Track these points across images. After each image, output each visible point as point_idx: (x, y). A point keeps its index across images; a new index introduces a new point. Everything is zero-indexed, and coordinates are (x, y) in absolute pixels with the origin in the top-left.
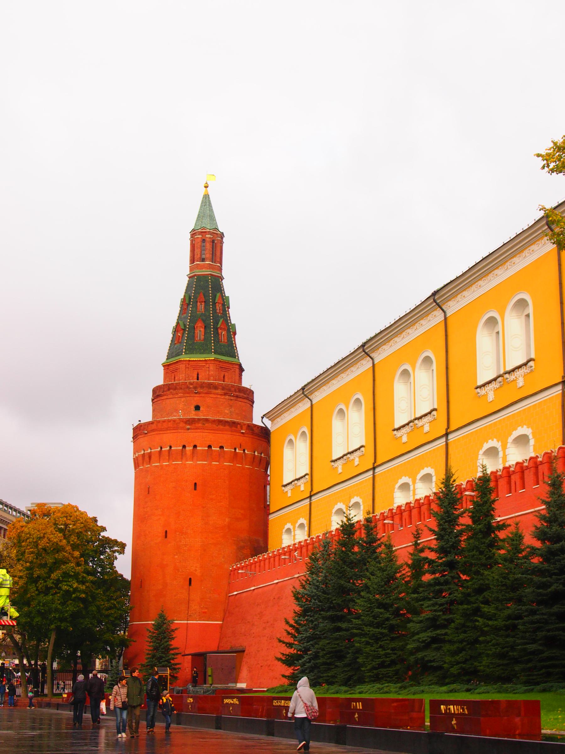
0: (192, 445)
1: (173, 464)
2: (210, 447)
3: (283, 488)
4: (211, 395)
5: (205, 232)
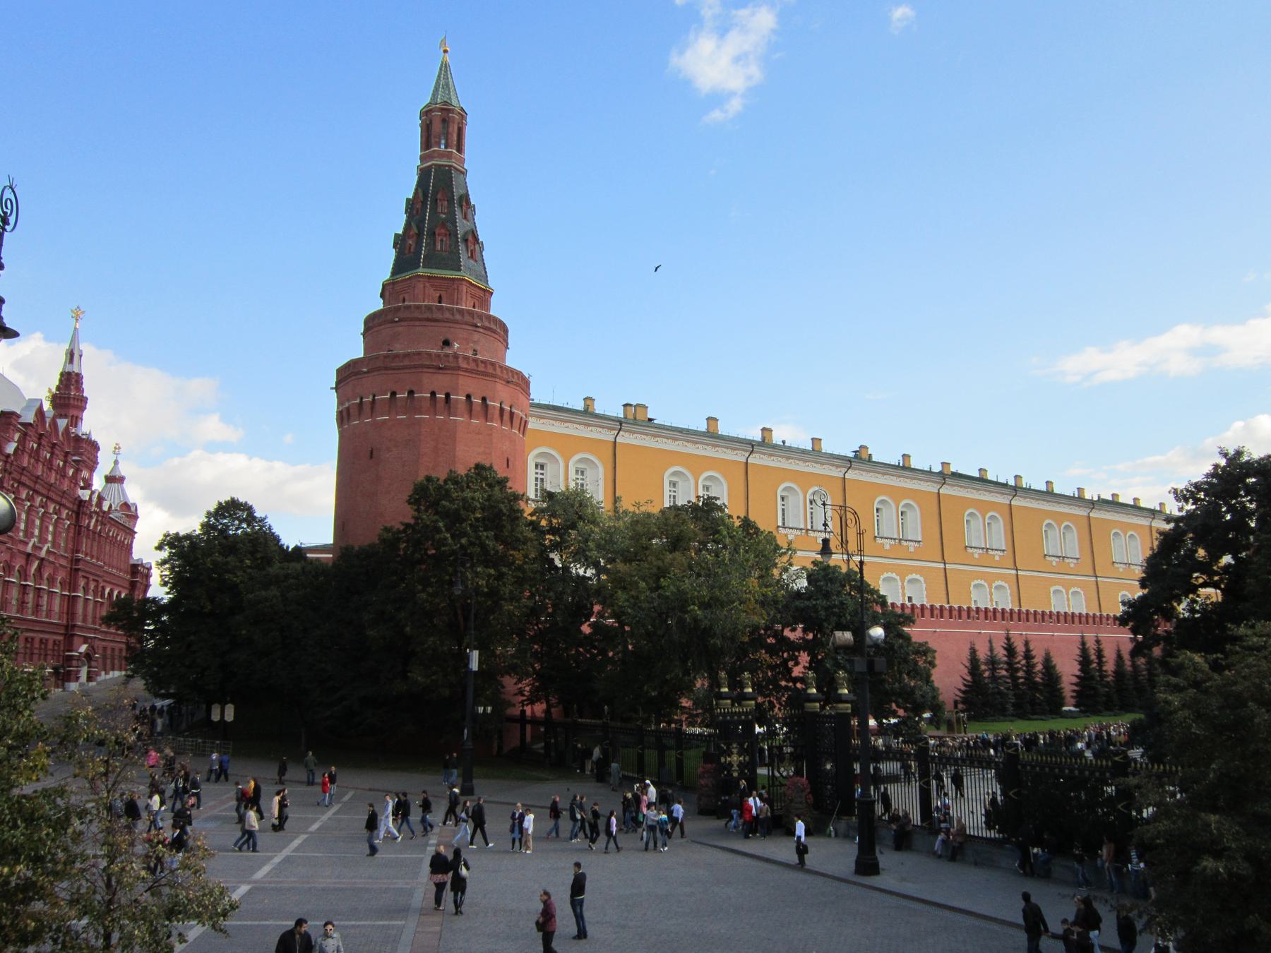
5: (449, 110)
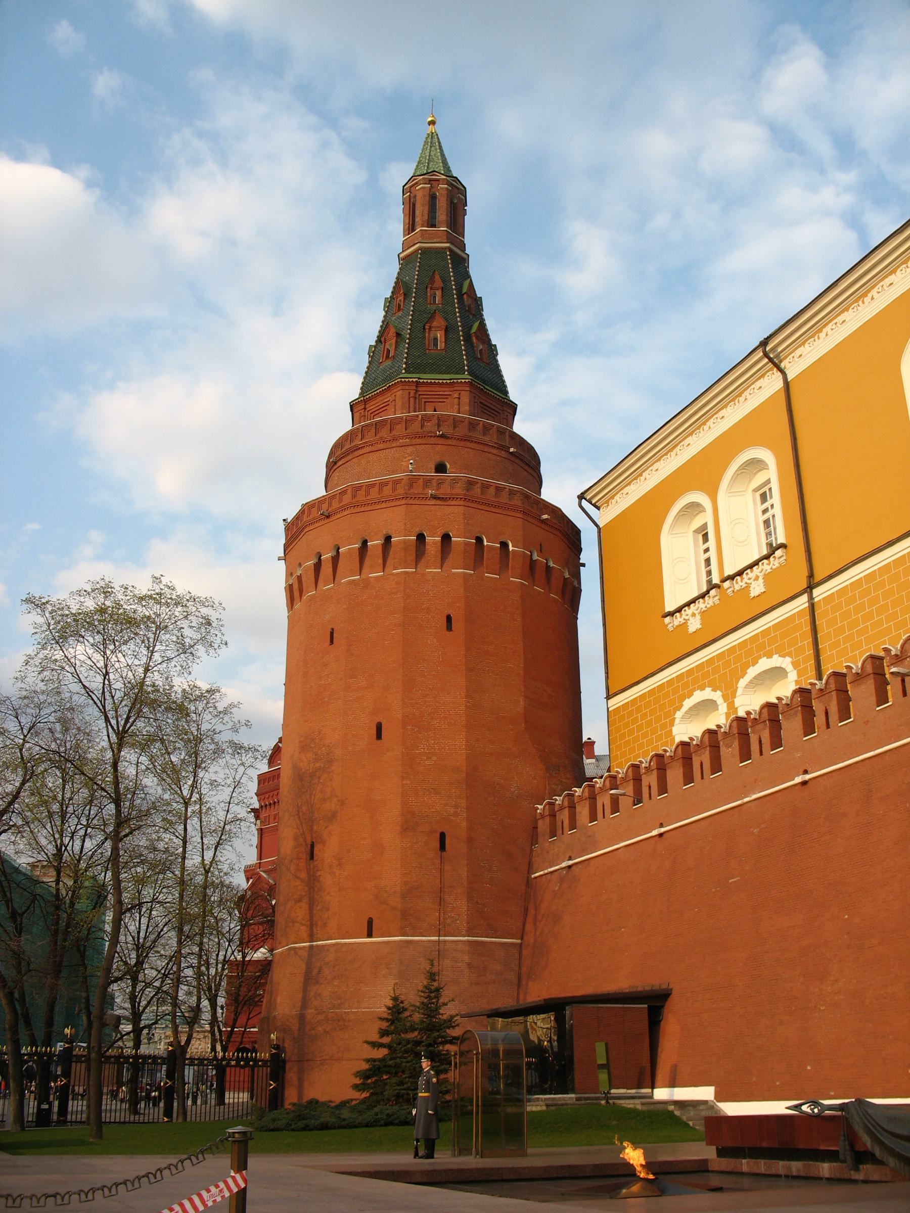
0: (441, 532)
1: (393, 575)
2: (479, 540)
3: (667, 620)
4: (468, 444)
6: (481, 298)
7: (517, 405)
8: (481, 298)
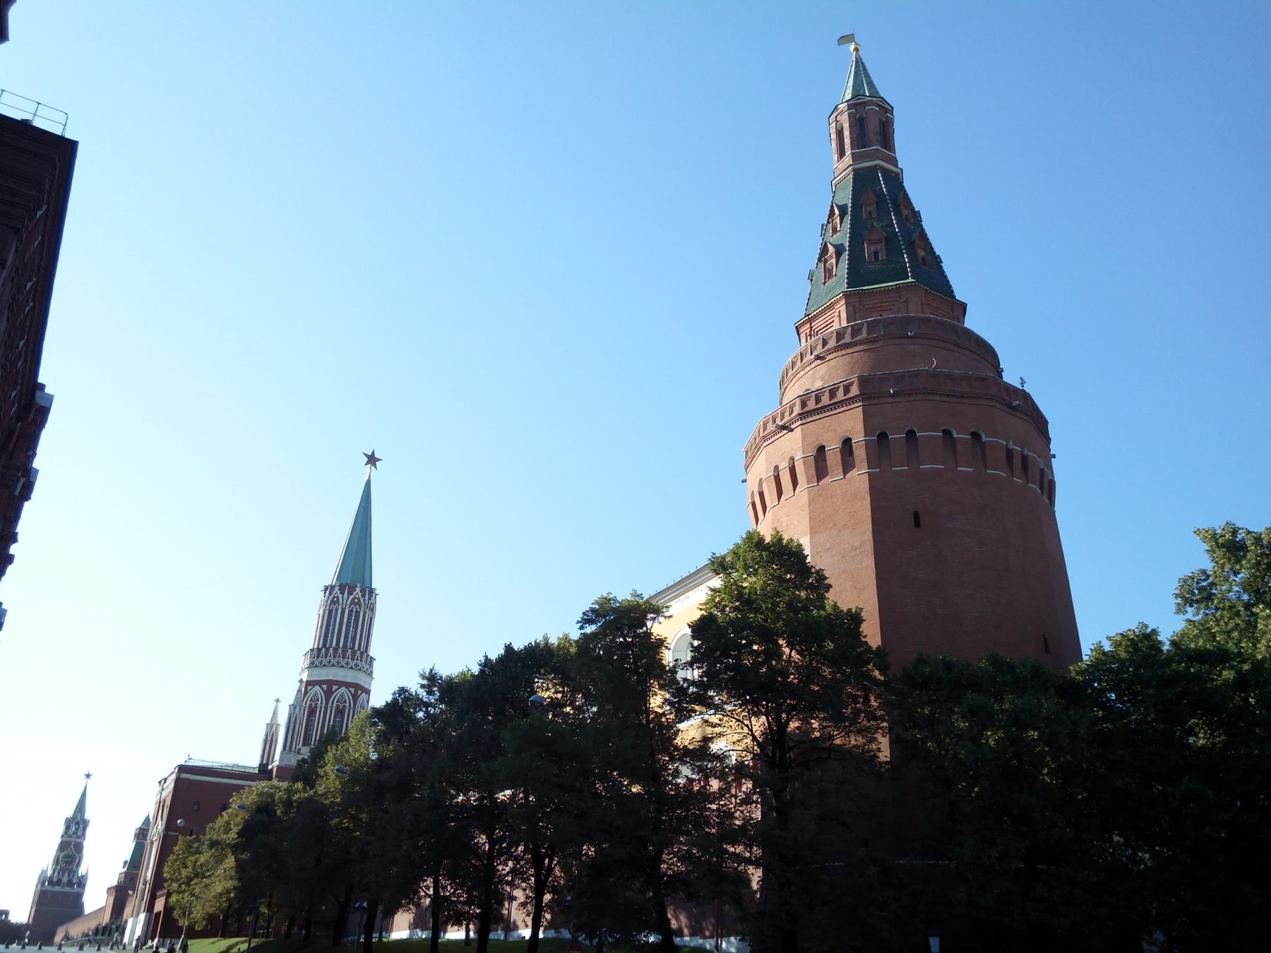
2: (947, 433)
6: (919, 211)
7: (966, 304)
8: (919, 211)
